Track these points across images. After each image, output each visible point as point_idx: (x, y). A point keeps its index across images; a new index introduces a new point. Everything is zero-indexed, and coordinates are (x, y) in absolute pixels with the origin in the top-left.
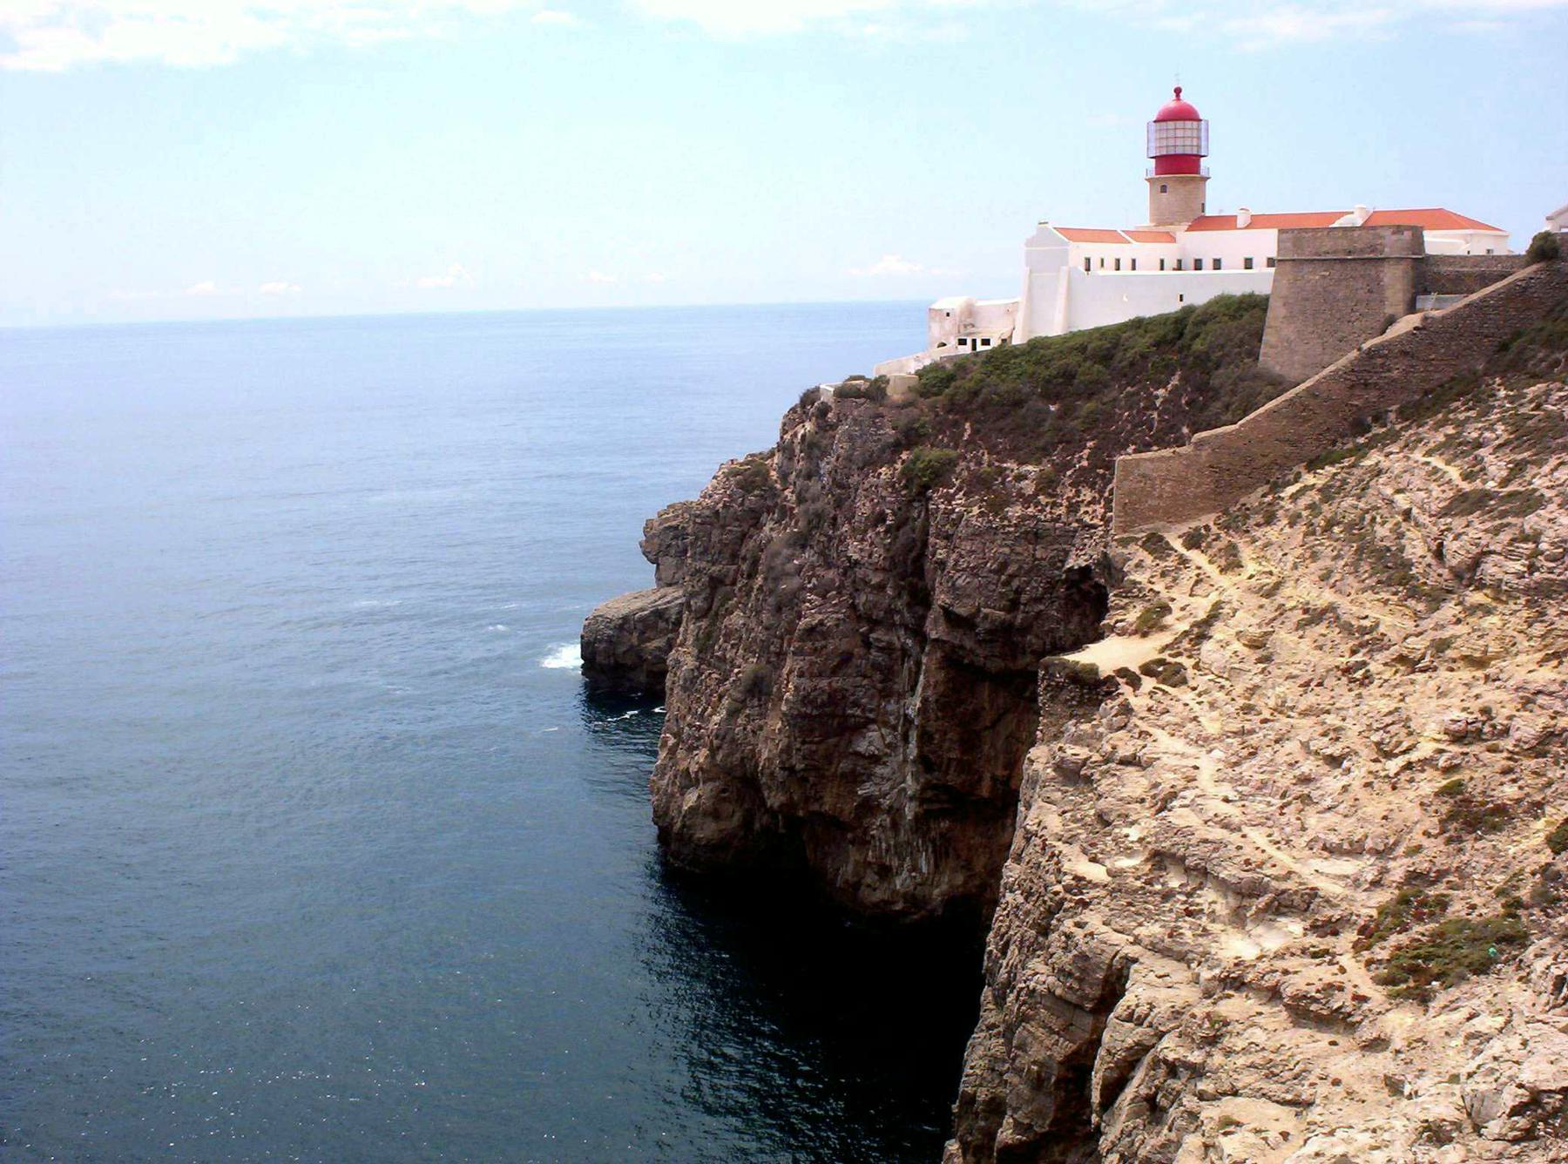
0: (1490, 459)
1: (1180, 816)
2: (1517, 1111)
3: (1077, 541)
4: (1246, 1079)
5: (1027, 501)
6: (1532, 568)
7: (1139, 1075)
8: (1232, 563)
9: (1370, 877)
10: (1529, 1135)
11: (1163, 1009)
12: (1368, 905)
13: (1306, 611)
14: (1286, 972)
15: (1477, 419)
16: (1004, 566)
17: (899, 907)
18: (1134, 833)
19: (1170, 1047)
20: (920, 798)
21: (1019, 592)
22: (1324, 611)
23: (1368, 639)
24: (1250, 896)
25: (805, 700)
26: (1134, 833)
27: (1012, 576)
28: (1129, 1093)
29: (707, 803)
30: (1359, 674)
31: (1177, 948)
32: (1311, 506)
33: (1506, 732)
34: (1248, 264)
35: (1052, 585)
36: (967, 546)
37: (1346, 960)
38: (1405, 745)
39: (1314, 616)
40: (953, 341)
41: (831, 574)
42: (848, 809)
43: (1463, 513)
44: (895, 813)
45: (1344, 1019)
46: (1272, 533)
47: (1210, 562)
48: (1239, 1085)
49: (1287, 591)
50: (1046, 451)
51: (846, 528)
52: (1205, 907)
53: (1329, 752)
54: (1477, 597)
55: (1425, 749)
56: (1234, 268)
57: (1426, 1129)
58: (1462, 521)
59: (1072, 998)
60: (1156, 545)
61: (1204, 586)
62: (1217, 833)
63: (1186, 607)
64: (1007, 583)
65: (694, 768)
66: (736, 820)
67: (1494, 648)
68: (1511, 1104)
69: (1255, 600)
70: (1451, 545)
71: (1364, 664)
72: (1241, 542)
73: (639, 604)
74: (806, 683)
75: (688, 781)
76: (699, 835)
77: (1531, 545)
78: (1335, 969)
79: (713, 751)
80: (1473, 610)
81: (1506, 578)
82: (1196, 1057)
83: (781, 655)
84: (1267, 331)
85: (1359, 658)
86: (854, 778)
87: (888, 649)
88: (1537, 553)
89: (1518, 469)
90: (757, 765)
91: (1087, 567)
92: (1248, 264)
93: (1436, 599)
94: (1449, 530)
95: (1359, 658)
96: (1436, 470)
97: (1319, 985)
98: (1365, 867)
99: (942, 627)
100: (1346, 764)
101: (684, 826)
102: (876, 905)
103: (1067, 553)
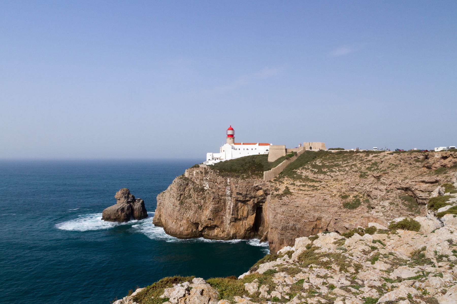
0: (313, 169)
4: (346, 217)
23: (314, 186)
25: (214, 208)
34: (244, 149)
40: (211, 159)
41: (213, 190)
46: (286, 178)
54: (326, 181)
55: (335, 193)
56: (242, 149)
73: (119, 207)
92: (244, 149)
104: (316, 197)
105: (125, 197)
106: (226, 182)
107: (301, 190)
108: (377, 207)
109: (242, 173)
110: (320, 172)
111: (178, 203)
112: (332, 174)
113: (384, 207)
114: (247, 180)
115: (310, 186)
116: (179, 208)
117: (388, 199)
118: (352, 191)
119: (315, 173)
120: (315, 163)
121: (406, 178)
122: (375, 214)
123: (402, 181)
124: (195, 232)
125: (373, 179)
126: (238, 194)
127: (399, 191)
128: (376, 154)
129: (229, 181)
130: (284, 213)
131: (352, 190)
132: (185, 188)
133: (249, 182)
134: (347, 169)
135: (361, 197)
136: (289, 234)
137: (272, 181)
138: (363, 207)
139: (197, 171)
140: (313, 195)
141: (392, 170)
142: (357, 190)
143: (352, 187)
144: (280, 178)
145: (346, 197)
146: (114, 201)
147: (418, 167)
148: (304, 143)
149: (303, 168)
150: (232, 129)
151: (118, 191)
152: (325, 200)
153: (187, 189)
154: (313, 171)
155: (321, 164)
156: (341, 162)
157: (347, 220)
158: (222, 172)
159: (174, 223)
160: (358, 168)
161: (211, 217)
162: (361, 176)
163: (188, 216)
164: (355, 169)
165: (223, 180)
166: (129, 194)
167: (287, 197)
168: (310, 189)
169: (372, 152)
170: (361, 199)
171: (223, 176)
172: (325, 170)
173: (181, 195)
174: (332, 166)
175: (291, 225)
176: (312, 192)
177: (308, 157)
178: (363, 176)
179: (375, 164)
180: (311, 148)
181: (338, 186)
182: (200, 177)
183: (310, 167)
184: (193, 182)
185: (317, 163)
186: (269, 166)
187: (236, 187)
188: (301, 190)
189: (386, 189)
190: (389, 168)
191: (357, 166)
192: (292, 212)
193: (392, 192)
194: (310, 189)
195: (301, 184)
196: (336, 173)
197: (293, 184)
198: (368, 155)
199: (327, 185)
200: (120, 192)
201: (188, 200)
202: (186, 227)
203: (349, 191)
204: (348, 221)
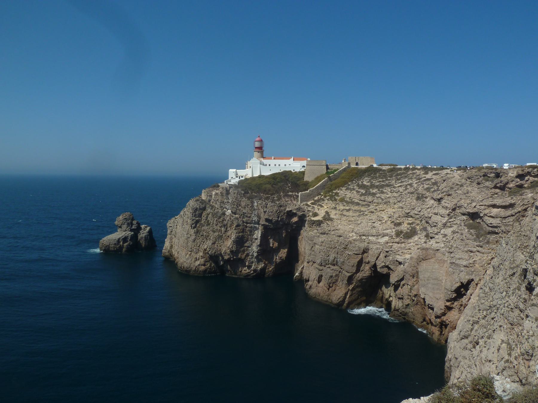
7: (381, 254)
17: (252, 272)
20: (258, 252)
23: (360, 211)
25: (237, 238)
29: (203, 263)
34: (275, 165)
35: (284, 213)
40: (234, 177)
41: (237, 216)
42: (243, 256)
44: (253, 255)
55: (386, 219)
60: (307, 205)
66: (208, 265)
73: (121, 236)
74: (237, 235)
75: (196, 259)
76: (200, 269)
87: (251, 227)
92: (275, 165)
93: (369, 206)
104: (362, 224)
105: (128, 224)
106: (252, 206)
107: (345, 216)
108: (437, 237)
109: (272, 194)
110: (368, 193)
111: (192, 231)
112: (383, 196)
113: (445, 235)
114: (278, 203)
115: (355, 210)
116: (194, 237)
117: (451, 227)
118: (407, 217)
119: (361, 195)
120: (362, 182)
121: (473, 201)
122: (435, 246)
123: (468, 204)
125: (432, 202)
126: (267, 220)
127: (465, 217)
128: (437, 172)
129: (256, 204)
130: (323, 244)
131: (408, 215)
132: (202, 213)
133: (281, 206)
134: (401, 189)
135: (418, 225)
136: (329, 270)
137: (309, 203)
138: (419, 236)
139: (217, 192)
140: (359, 222)
141: (455, 191)
142: (413, 215)
143: (407, 211)
146: (113, 229)
147: (488, 187)
148: (350, 158)
149: (347, 189)
150: (261, 141)
151: (119, 216)
153: (204, 214)
154: (359, 192)
155: (369, 184)
156: (394, 182)
157: (400, 253)
158: (248, 193)
159: (188, 256)
160: (414, 189)
161: (234, 249)
162: (418, 199)
163: (205, 247)
164: (411, 190)
165: (249, 202)
166: (133, 219)
167: (328, 224)
168: (355, 214)
169: (432, 169)
170: (418, 227)
171: (249, 198)
172: (374, 191)
173: (197, 222)
174: (383, 186)
175: (331, 258)
176: (358, 218)
177: (353, 175)
178: (420, 198)
179: (435, 183)
180: (357, 164)
181: (390, 211)
182: (220, 198)
183: (355, 187)
184: (210, 205)
185: (365, 183)
186: (306, 186)
188: (345, 216)
189: (449, 215)
190: (452, 188)
191: (412, 186)
192: (332, 242)
193: (455, 218)
194: (355, 214)
195: (345, 208)
197: (335, 208)
198: (426, 173)
199: (376, 209)
200: (121, 217)
201: (205, 228)
203: (402, 217)
204: (401, 254)
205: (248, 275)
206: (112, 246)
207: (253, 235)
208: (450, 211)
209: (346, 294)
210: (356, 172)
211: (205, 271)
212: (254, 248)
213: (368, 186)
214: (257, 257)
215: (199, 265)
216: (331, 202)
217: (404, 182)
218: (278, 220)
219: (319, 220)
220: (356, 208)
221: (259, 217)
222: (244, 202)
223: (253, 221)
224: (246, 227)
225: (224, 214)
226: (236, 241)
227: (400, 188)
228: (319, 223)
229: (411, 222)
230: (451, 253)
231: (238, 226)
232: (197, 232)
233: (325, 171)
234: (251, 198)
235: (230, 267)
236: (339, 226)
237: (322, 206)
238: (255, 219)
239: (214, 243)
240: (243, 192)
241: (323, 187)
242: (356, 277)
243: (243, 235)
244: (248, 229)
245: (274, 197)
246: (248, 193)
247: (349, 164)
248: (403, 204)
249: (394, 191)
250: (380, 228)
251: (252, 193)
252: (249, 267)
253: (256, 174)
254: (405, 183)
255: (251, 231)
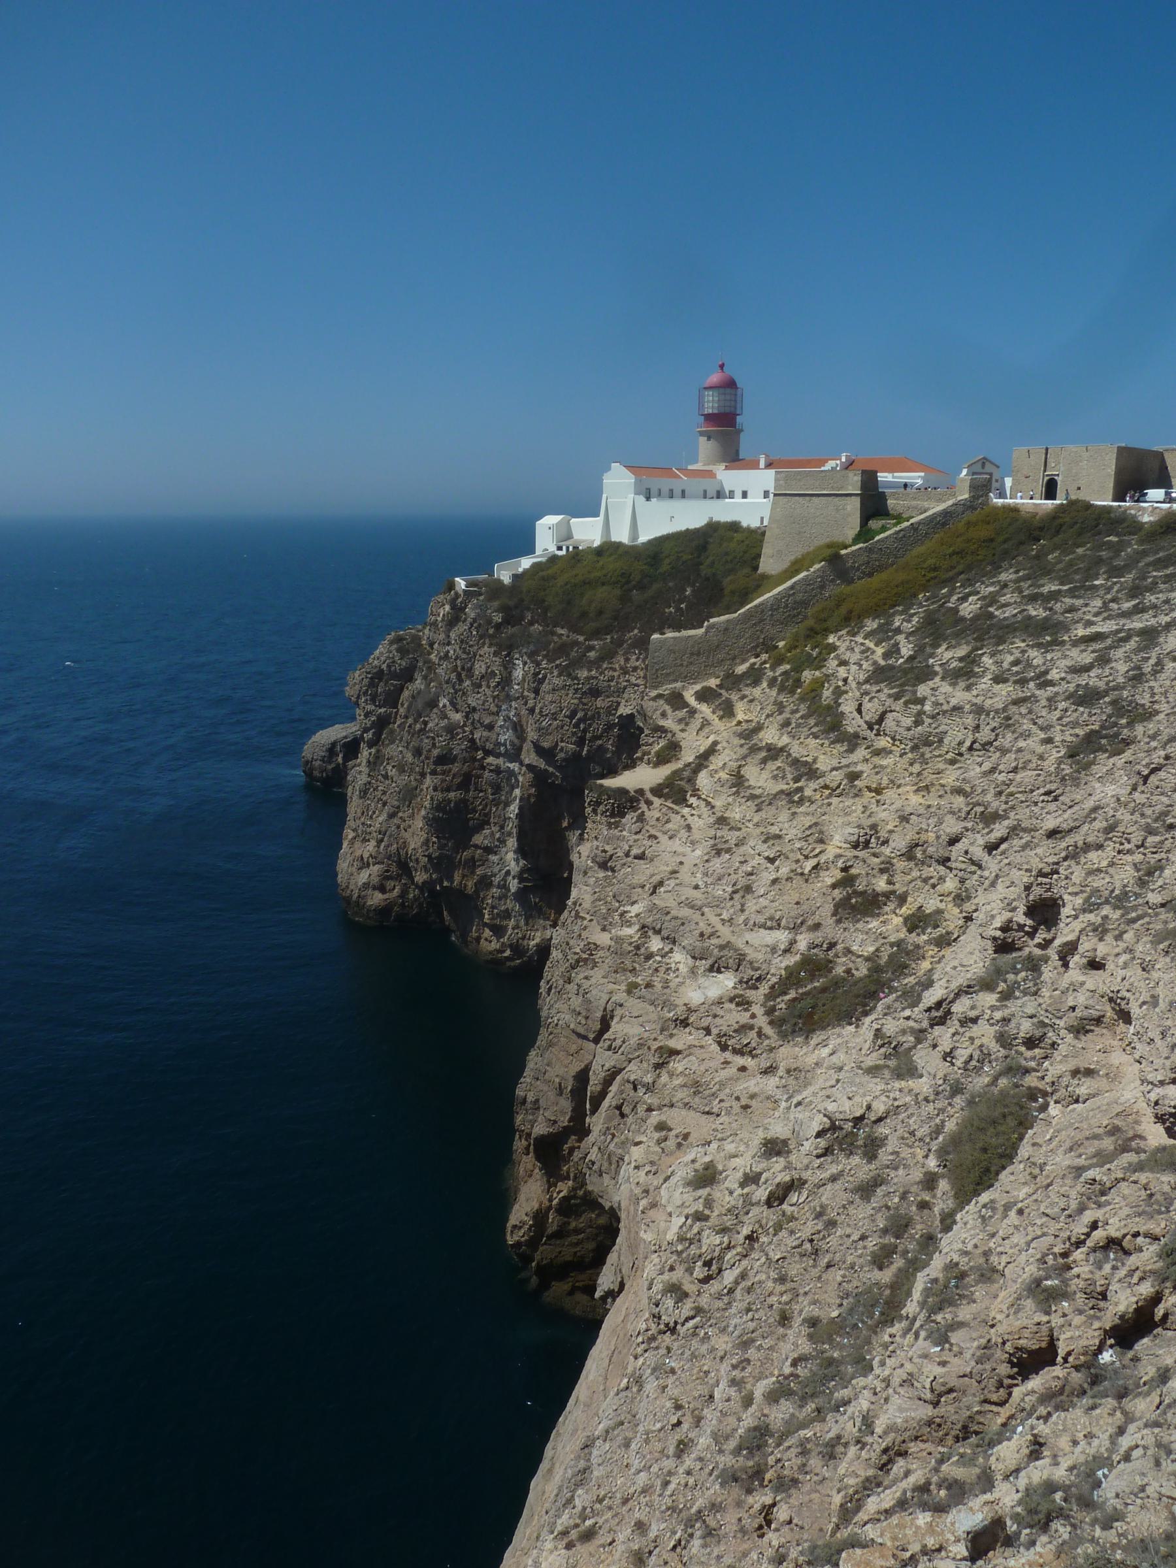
1: (664, 899)
2: (819, 1135)
3: (626, 695)
5: (591, 665)
6: (918, 723)
7: (614, 1088)
8: (728, 711)
9: (783, 947)
10: (827, 1152)
11: (633, 1041)
12: (780, 965)
13: (769, 750)
14: (715, 1016)
15: (901, 613)
16: (574, 713)
17: (508, 953)
18: (635, 910)
19: (634, 1071)
20: (521, 880)
21: (585, 731)
22: (782, 749)
23: (807, 770)
24: (701, 959)
25: (439, 807)
26: (635, 910)
27: (580, 720)
28: (606, 1103)
29: (375, 880)
30: (796, 798)
31: (648, 996)
32: (785, 673)
33: (883, 843)
35: (609, 727)
36: (549, 697)
37: (757, 1009)
38: (817, 851)
39: (774, 752)
40: (552, 548)
41: (457, 717)
43: (877, 683)
44: (504, 886)
45: (751, 1052)
46: (757, 692)
47: (714, 712)
48: (674, 1100)
49: (761, 735)
50: (608, 630)
51: (468, 683)
52: (673, 965)
53: (766, 854)
54: (883, 742)
55: (831, 851)
57: (765, 1145)
58: (875, 688)
59: (581, 1030)
60: (676, 700)
61: (706, 730)
62: (685, 912)
63: (692, 744)
64: (577, 726)
65: (366, 856)
67: (885, 782)
68: (816, 1130)
69: (737, 741)
70: (867, 706)
71: (800, 789)
72: (734, 697)
74: (440, 796)
76: (370, 903)
77: (919, 707)
78: (748, 1014)
79: (380, 841)
80: (878, 753)
81: (900, 730)
82: (648, 1079)
83: (423, 775)
84: (765, 545)
85: (799, 784)
86: (472, 864)
87: (497, 770)
88: (920, 713)
89: (920, 650)
90: (407, 853)
91: (632, 715)
93: (853, 741)
94: (867, 693)
95: (799, 784)
96: (868, 649)
97: (736, 1026)
98: (781, 937)
99: (533, 755)
100: (777, 863)
101: (359, 896)
102: (491, 953)
103: (619, 704)
106: (506, 681)
107: (738, 781)
109: (596, 634)
114: (583, 674)
115: (796, 762)
116: (363, 779)
118: (944, 861)
124: (416, 899)
129: (518, 673)
133: (595, 693)
144: (733, 682)
145: (858, 904)
148: (1018, 452)
150: (730, 385)
152: (748, 889)
153: (406, 694)
161: (434, 850)
167: (641, 818)
180: (1050, 490)
184: (430, 661)
187: (532, 711)
196: (968, 688)
197: (749, 733)
199: (854, 777)
202: (375, 869)
205: (495, 962)
206: (317, 764)
207: (507, 804)
208: (1020, 918)
209: (540, 1217)
210: (984, 532)
211: (384, 911)
212: (510, 860)
213: (963, 619)
214: (521, 895)
215: (366, 886)
216: (774, 693)
217: (1143, 610)
218: (576, 756)
219: (623, 792)
220: (809, 748)
221: (518, 728)
222: (486, 660)
223: (499, 744)
224: (483, 768)
225: (433, 704)
226: (435, 819)
227: (1074, 653)
228: (626, 802)
229: (931, 905)
230: (672, 1329)
231: (443, 759)
232: (375, 763)
233: (852, 527)
234: (506, 649)
235: (450, 913)
236: (676, 845)
237: (728, 711)
238: (506, 736)
239: (392, 816)
240: (498, 618)
241: (791, 608)
242: (577, 1155)
243: (464, 801)
244: (487, 774)
245: (591, 648)
246: (522, 618)
247: (982, 487)
248: (987, 766)
249: (1029, 665)
250: (752, 905)
251: (531, 623)
252: (498, 931)
253: (621, 535)
254: (1137, 624)
255: (497, 789)
